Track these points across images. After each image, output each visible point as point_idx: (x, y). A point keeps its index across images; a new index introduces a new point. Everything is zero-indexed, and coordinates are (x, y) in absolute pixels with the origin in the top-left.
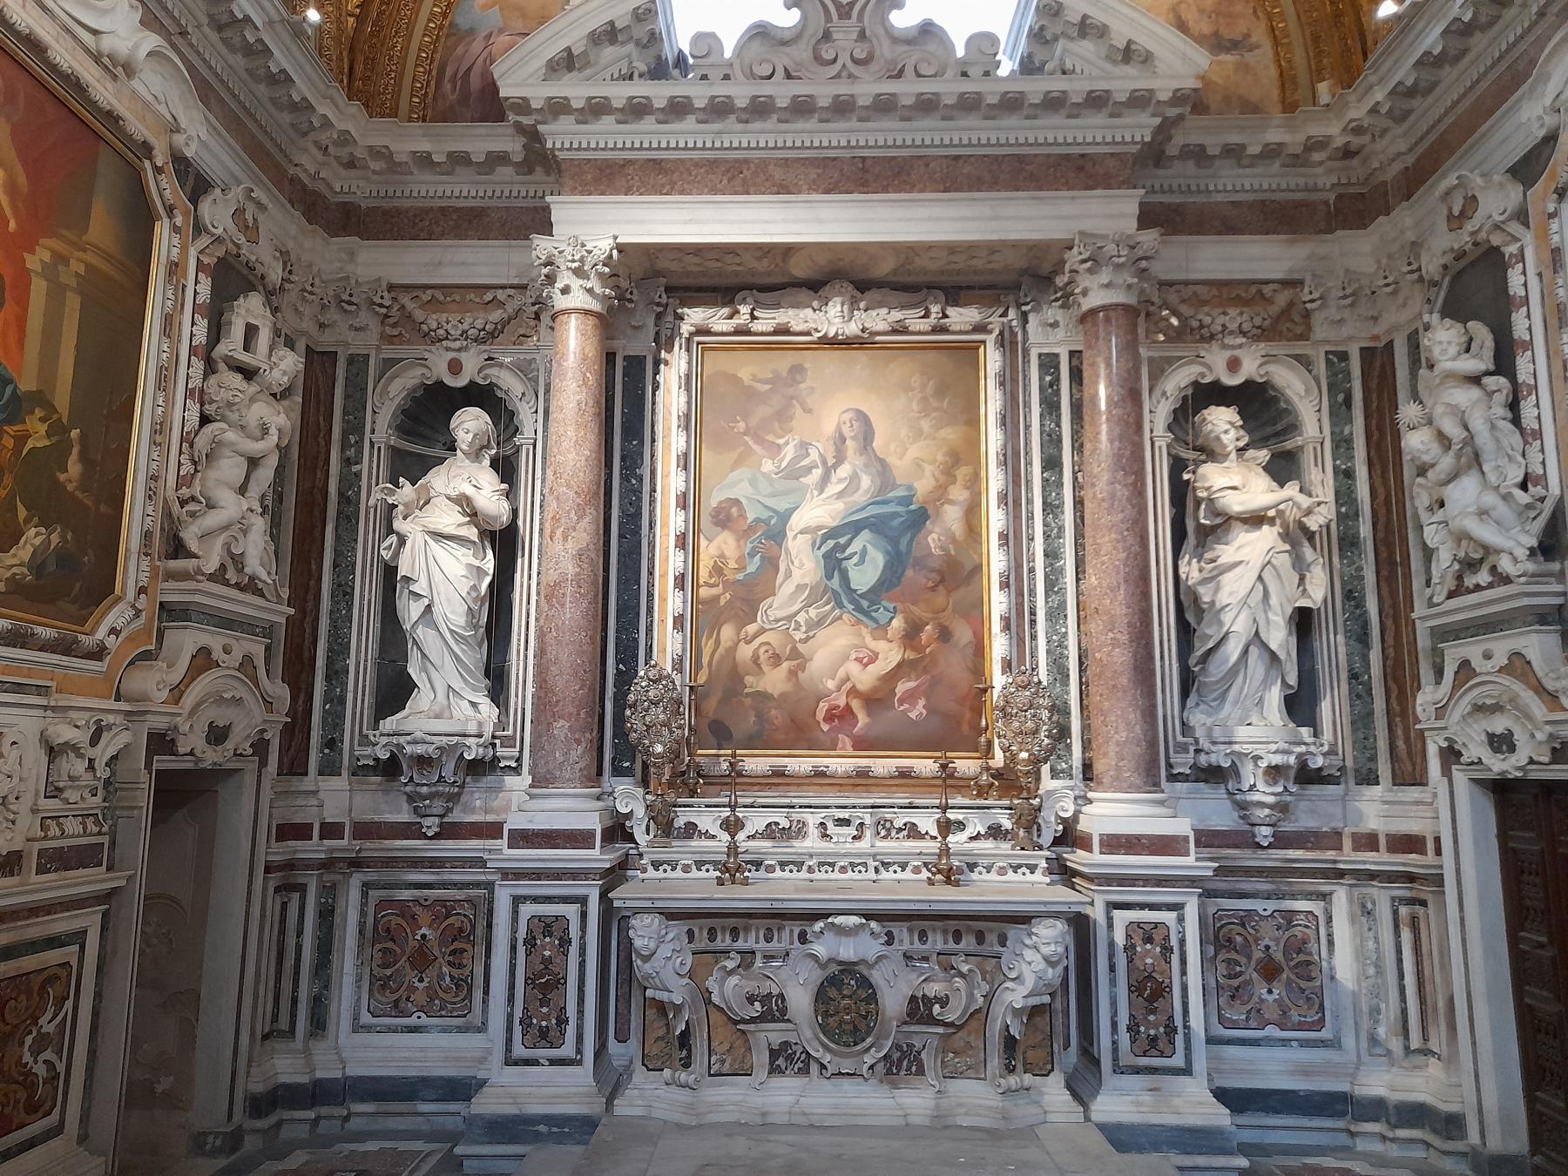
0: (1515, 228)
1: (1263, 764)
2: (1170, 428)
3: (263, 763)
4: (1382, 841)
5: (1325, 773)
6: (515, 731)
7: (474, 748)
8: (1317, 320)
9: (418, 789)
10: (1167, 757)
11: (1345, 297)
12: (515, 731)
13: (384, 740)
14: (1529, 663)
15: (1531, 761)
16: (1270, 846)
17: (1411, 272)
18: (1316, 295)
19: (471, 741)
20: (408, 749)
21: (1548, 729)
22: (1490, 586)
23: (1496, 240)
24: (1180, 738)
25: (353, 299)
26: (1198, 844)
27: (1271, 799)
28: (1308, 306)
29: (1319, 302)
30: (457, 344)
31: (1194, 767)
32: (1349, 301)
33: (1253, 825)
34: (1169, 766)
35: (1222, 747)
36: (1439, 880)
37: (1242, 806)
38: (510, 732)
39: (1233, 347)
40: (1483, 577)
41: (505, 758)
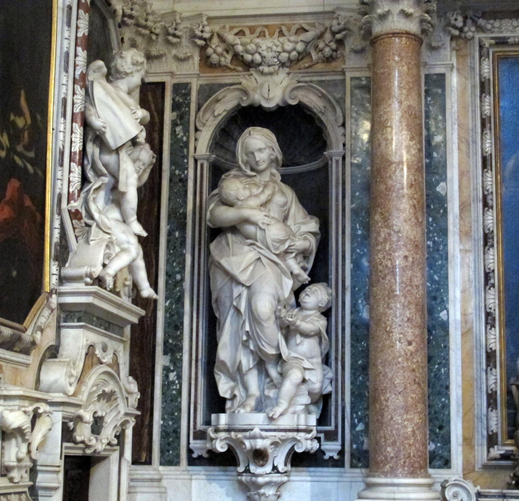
3: (121, 455)
6: (336, 427)
7: (303, 441)
9: (254, 479)
12: (336, 427)
13: (223, 435)
19: (301, 436)
20: (248, 444)
25: (178, 33)
30: (271, 69)
38: (332, 428)
41: (330, 451)
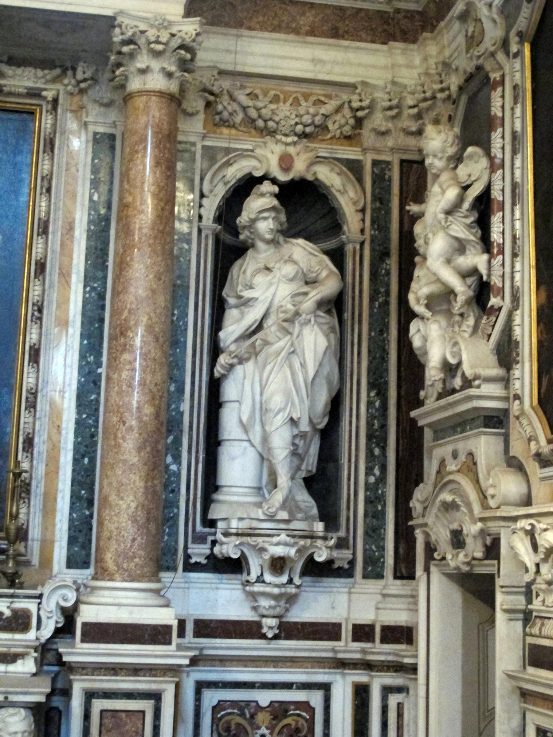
0: (501, 56)
1: (267, 557)
2: (218, 219)
4: (378, 630)
5: (336, 566)
8: (368, 126)
10: (186, 548)
11: (390, 108)
14: (475, 464)
15: (474, 559)
16: (276, 637)
17: (442, 90)
18: (366, 103)
21: (479, 525)
22: (463, 388)
23: (488, 67)
24: (199, 528)
26: (181, 633)
27: (276, 591)
28: (360, 114)
29: (367, 111)
31: (211, 557)
32: (393, 112)
33: (264, 616)
34: (187, 557)
35: (233, 538)
36: (414, 669)
37: (253, 596)
39: (287, 144)
40: (457, 382)
